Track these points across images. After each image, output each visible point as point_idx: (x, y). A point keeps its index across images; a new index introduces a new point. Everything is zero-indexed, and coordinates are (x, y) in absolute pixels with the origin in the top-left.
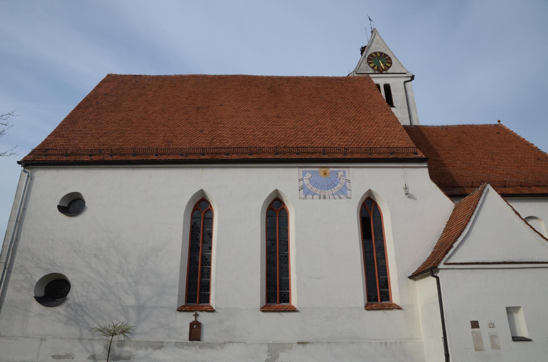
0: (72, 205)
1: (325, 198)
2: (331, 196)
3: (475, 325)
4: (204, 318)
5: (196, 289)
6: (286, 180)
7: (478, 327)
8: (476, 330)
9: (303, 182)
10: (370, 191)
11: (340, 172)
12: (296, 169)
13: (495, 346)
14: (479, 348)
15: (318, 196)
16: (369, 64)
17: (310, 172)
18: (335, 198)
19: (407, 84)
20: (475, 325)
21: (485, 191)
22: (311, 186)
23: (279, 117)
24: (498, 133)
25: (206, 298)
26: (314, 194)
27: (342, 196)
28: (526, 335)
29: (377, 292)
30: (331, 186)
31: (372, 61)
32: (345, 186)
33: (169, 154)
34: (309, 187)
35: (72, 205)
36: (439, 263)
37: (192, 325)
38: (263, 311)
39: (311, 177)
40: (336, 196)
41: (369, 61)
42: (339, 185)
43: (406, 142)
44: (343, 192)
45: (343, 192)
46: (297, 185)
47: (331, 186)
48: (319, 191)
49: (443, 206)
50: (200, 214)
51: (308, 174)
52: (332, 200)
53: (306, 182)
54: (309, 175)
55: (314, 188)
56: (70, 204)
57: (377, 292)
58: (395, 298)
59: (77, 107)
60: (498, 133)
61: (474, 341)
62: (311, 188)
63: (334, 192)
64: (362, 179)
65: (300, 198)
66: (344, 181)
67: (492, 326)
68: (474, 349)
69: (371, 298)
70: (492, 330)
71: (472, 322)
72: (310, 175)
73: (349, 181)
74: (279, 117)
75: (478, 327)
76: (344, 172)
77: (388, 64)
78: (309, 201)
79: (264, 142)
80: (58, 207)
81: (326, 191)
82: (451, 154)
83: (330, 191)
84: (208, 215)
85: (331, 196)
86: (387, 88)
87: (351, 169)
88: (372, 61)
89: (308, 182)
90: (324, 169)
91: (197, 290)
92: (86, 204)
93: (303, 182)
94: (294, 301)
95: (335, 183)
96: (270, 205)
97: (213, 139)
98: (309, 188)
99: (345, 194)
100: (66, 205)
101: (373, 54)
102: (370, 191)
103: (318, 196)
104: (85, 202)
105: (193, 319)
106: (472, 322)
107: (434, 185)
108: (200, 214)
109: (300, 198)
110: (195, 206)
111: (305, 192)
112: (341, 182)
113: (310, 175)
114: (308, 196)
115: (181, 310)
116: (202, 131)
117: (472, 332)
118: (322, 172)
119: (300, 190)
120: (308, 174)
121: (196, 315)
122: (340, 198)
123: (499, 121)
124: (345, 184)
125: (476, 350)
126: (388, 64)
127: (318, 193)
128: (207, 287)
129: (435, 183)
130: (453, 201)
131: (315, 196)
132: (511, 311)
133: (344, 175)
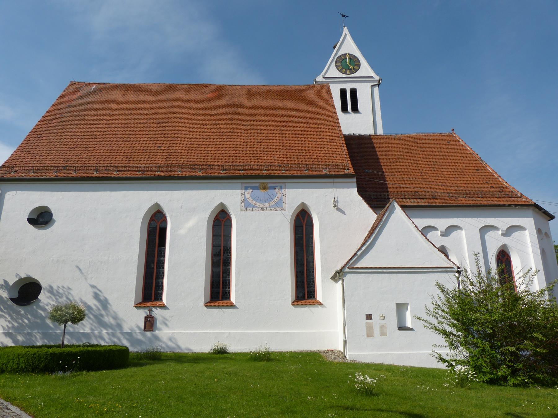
0: (41, 218)
2: (268, 209)
4: (157, 313)
7: (371, 319)
8: (369, 321)
10: (303, 204)
13: (383, 334)
14: (370, 335)
18: (271, 210)
20: (369, 317)
21: (390, 207)
23: (233, 132)
25: (159, 297)
26: (254, 207)
27: (277, 208)
28: (411, 327)
29: (305, 291)
32: (281, 200)
33: (127, 171)
35: (41, 218)
37: (146, 318)
38: (206, 306)
40: (273, 209)
42: (276, 199)
43: (342, 157)
45: (279, 205)
52: (269, 212)
55: (254, 202)
56: (38, 216)
57: (305, 291)
58: (319, 296)
59: (41, 120)
61: (367, 329)
62: (252, 201)
65: (241, 210)
68: (366, 336)
71: (367, 315)
74: (233, 132)
75: (371, 319)
77: (356, 67)
78: (249, 213)
79: (215, 158)
80: (28, 219)
81: (265, 204)
84: (163, 225)
85: (268, 209)
86: (354, 92)
89: (249, 196)
91: (151, 290)
92: (54, 217)
94: (233, 298)
95: (272, 197)
96: (217, 216)
97: (169, 155)
98: (250, 201)
100: (35, 217)
101: (342, 57)
102: (303, 204)
104: (52, 214)
106: (367, 315)
109: (241, 210)
110: (152, 217)
111: (246, 205)
114: (248, 208)
115: (138, 306)
116: (160, 147)
119: (241, 203)
121: (150, 311)
122: (276, 210)
124: (282, 198)
125: (368, 336)
126: (356, 67)
128: (160, 287)
129: (362, 196)
130: (376, 213)
131: (254, 209)
132: (401, 307)
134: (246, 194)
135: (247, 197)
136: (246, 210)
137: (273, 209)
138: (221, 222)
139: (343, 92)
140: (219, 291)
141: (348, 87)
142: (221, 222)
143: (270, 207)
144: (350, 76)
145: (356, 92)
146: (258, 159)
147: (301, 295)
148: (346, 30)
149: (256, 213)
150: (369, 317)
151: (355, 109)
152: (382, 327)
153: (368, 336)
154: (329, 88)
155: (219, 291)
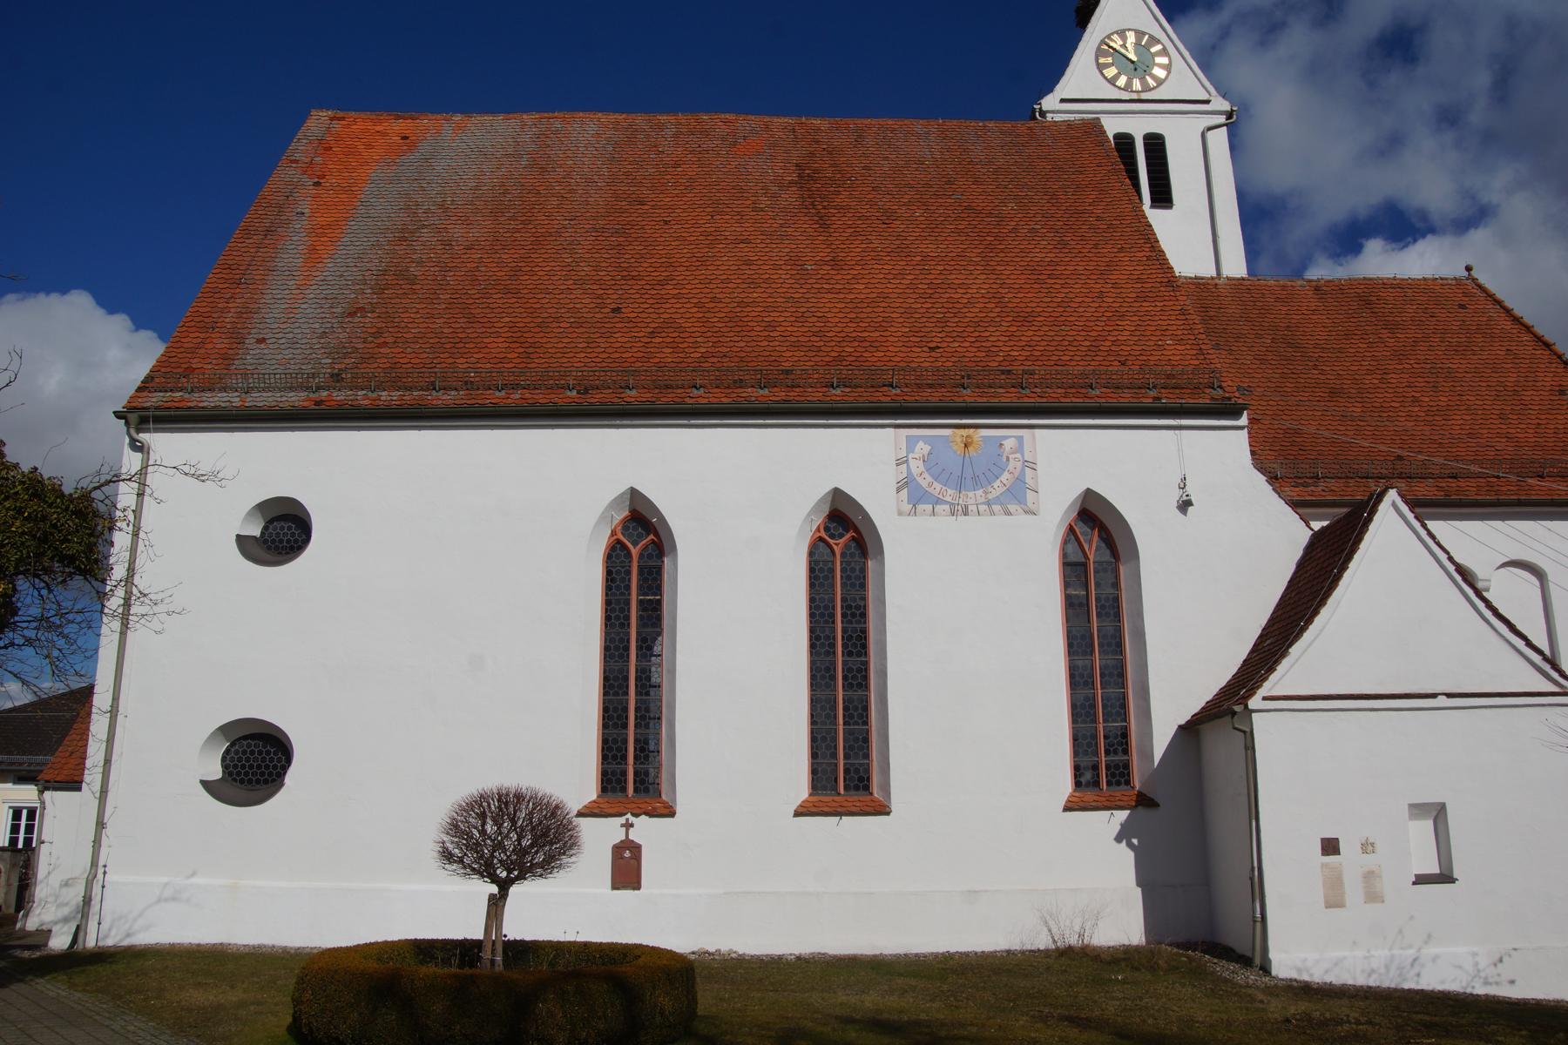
1: (966, 513)
3: (1330, 847)
4: (645, 830)
5: (624, 757)
6: (863, 459)
12: (891, 431)
13: (1373, 896)
14: (1334, 901)
15: (947, 507)
17: (925, 439)
18: (992, 513)
19: (1210, 135)
20: (1330, 847)
22: (929, 479)
24: (1462, 306)
26: (938, 501)
27: (1012, 508)
31: (1110, 60)
32: (1020, 480)
34: (925, 481)
35: (282, 532)
36: (1251, 693)
37: (618, 850)
41: (1102, 60)
42: (1005, 477)
44: (1018, 495)
46: (892, 475)
48: (950, 492)
50: (638, 559)
51: (921, 444)
53: (916, 467)
54: (922, 448)
55: (938, 486)
60: (1462, 306)
62: (930, 485)
64: (1072, 459)
65: (900, 513)
66: (1019, 464)
67: (1367, 847)
69: (1083, 780)
70: (1370, 861)
71: (1323, 840)
72: (927, 448)
76: (1020, 439)
81: (971, 494)
82: (1322, 372)
83: (980, 492)
85: (982, 508)
86: (1156, 145)
88: (1110, 60)
89: (922, 468)
90: (965, 432)
98: (924, 484)
99: (1021, 501)
102: (1089, 494)
103: (947, 507)
105: (619, 835)
106: (1323, 840)
107: (1260, 479)
108: (638, 559)
111: (915, 495)
112: (1011, 466)
113: (927, 448)
114: (920, 507)
117: (1323, 865)
119: (898, 490)
120: (921, 444)
121: (628, 826)
122: (1008, 513)
123: (1468, 269)
124: (1023, 472)
131: (939, 508)
133: (1020, 448)
134: (913, 464)
135: (915, 471)
136: (914, 512)
137: (996, 508)
138: (844, 549)
140: (845, 765)
142: (844, 549)
143: (988, 503)
144: (1144, 96)
147: (1088, 776)
149: (943, 523)
152: (1370, 876)
155: (845, 765)
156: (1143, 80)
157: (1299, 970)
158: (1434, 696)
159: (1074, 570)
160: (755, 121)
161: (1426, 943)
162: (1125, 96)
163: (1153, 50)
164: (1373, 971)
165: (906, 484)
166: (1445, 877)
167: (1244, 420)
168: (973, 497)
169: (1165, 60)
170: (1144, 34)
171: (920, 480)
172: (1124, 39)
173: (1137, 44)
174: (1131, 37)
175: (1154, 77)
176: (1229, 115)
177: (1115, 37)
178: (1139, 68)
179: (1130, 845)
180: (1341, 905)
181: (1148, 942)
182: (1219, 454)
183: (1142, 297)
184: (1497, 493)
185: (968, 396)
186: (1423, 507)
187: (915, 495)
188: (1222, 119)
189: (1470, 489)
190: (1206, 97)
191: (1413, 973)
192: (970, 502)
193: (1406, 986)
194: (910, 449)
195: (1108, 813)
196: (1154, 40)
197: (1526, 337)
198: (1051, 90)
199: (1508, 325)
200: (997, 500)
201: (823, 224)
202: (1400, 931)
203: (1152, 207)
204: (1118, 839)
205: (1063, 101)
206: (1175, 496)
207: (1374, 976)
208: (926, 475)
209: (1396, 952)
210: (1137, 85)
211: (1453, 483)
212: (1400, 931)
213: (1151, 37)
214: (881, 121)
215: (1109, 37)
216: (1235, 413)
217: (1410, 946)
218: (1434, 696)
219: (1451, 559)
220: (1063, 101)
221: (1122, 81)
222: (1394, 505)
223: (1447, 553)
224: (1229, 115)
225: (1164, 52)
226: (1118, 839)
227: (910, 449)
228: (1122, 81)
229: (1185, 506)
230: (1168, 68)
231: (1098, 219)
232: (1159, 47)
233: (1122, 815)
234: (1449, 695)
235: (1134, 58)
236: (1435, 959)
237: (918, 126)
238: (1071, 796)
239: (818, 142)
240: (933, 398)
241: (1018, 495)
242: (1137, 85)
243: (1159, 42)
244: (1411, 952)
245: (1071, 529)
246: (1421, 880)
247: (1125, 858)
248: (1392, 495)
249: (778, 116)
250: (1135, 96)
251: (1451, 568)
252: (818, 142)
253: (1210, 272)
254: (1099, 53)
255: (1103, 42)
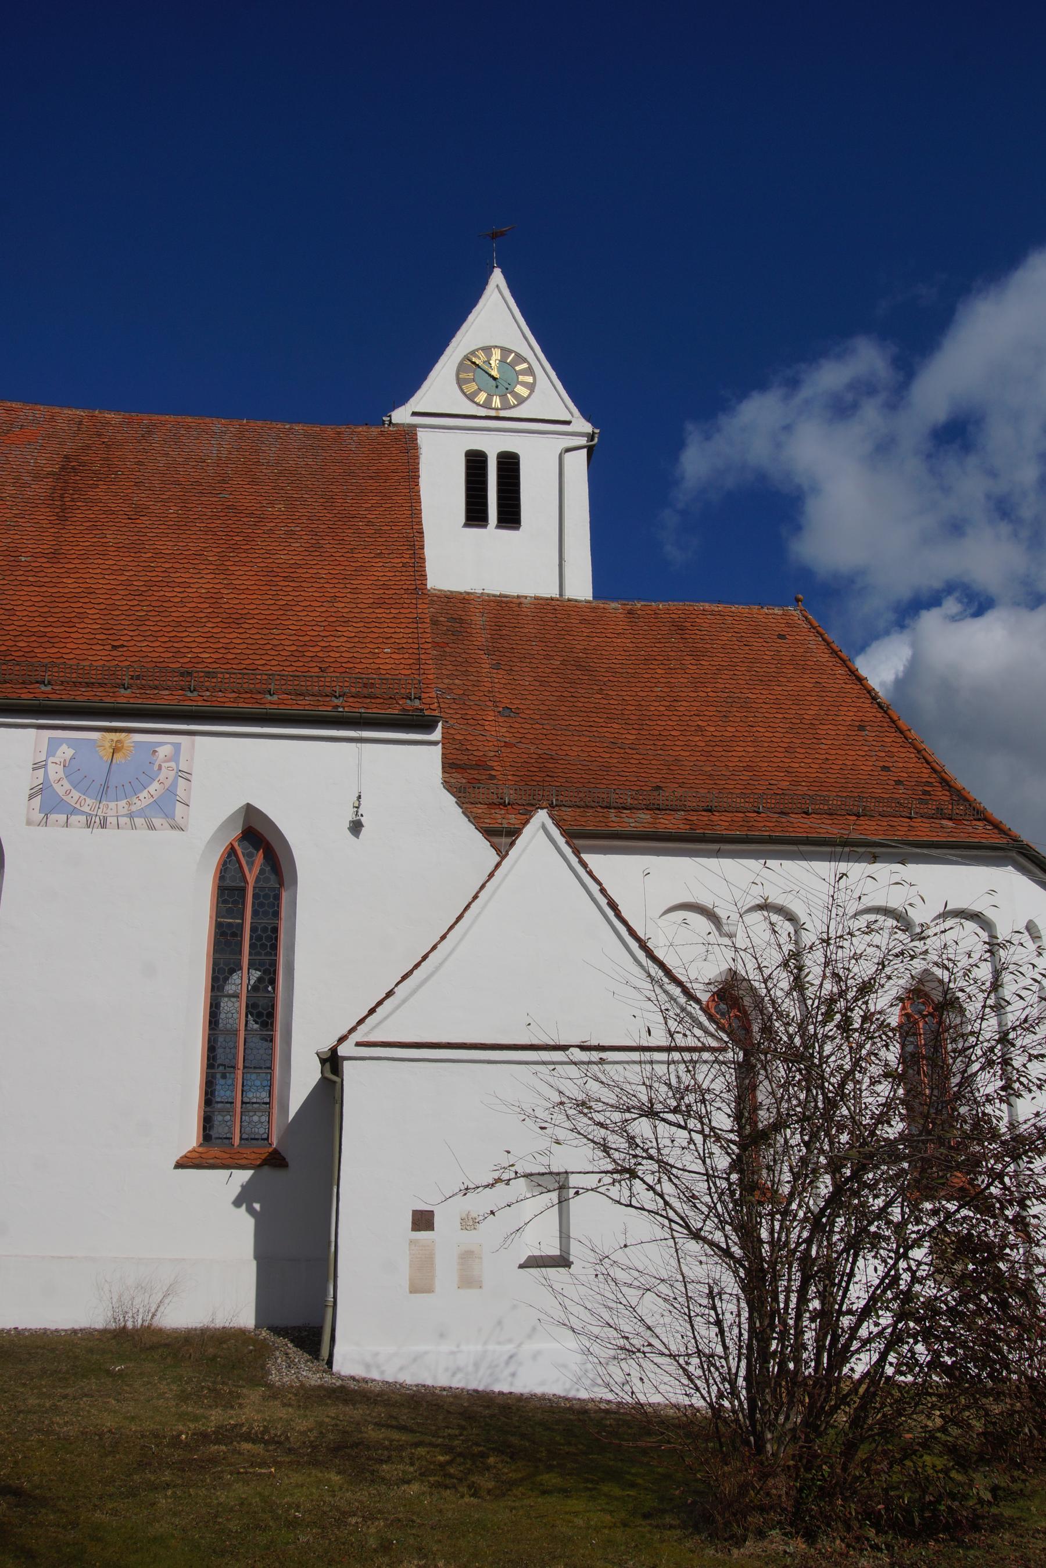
1: (103, 825)
2: (123, 820)
3: (423, 1221)
9: (46, 772)
10: (250, 811)
11: (164, 745)
12: (33, 731)
13: (468, 1281)
16: (460, 382)
17: (70, 743)
18: (134, 827)
22: (67, 786)
24: (781, 637)
26: (74, 811)
27: (157, 822)
30: (128, 787)
32: (171, 791)
39: (73, 758)
42: (154, 787)
44: (166, 809)
46: (28, 780)
47: (128, 787)
48: (89, 801)
49: (498, 859)
51: (64, 747)
53: (55, 771)
54: (65, 752)
55: (76, 794)
60: (781, 637)
62: (68, 793)
63: (134, 808)
64: (228, 770)
65: (29, 823)
66: (172, 774)
71: (416, 1213)
72: (70, 752)
73: (186, 776)
76: (177, 747)
81: (112, 805)
85: (123, 820)
86: (509, 464)
87: (198, 739)
89: (61, 774)
93: (46, 772)
98: (61, 791)
106: (416, 1213)
109: (29, 823)
111: (49, 803)
112: (162, 777)
113: (70, 752)
114: (53, 817)
118: (107, 744)
119: (31, 797)
120: (64, 747)
122: (152, 827)
124: (174, 784)
127: (86, 809)
131: (74, 819)
133: (175, 756)
135: (52, 777)
137: (139, 821)
139: (475, 462)
141: (492, 446)
143: (131, 816)
144: (502, 414)
145: (518, 464)
146: (115, 647)
148: (497, 277)
150: (423, 1221)
151: (510, 517)
152: (467, 1257)
153: (414, 1290)
154: (414, 438)
156: (503, 397)
157: (368, 1367)
158: (564, 1048)
159: (228, 893)
160: (42, 411)
161: (529, 1337)
162: (483, 412)
163: (518, 368)
164: (459, 1369)
165: (42, 791)
166: (562, 1261)
167: (437, 735)
168: (114, 808)
169: (529, 379)
170: (511, 351)
171: (57, 787)
172: (489, 356)
173: (503, 361)
174: (496, 355)
175: (516, 396)
176: (591, 437)
177: (481, 354)
178: (501, 386)
179: (251, 1211)
180: (429, 1289)
181: (257, 1327)
182: (406, 772)
183: (380, 603)
184: (750, 828)
185: (124, 697)
186: (583, 835)
187: (49, 803)
188: (583, 441)
189: (721, 824)
190: (568, 418)
191: (507, 1372)
192: (110, 813)
193: (497, 1388)
194: (51, 752)
195: (227, 1172)
196: (520, 358)
197: (841, 671)
198: (402, 399)
199: (825, 657)
200: (142, 813)
201: (62, 517)
202: (499, 1323)
203: (498, 527)
204: (237, 1203)
205: (414, 414)
206: (349, 816)
207: (459, 1376)
208: (65, 782)
209: (491, 1347)
210: (496, 402)
211: (705, 817)
212: (499, 1323)
213: (518, 355)
214: (179, 418)
215: (473, 353)
216: (426, 725)
217: (510, 1341)
218: (564, 1048)
219: (603, 891)
220: (414, 414)
221: (482, 397)
222: (544, 827)
223: (599, 883)
224: (591, 437)
225: (530, 371)
226: (237, 1203)
227: (51, 752)
228: (482, 397)
229: (356, 827)
230: (531, 387)
231: (369, 523)
232: (525, 366)
233: (244, 1176)
234: (583, 1048)
235: (495, 373)
236: (536, 1356)
237: (217, 425)
238: (194, 1151)
239: (100, 435)
240: (82, 697)
241: (166, 809)
242: (496, 402)
243: (525, 360)
244: (510, 1348)
245: (231, 851)
246: (535, 1262)
247: (244, 1224)
248: (542, 816)
249: (69, 407)
250: (493, 413)
251: (603, 902)
252: (100, 435)
253: (554, 593)
254: (461, 368)
255: (467, 358)
